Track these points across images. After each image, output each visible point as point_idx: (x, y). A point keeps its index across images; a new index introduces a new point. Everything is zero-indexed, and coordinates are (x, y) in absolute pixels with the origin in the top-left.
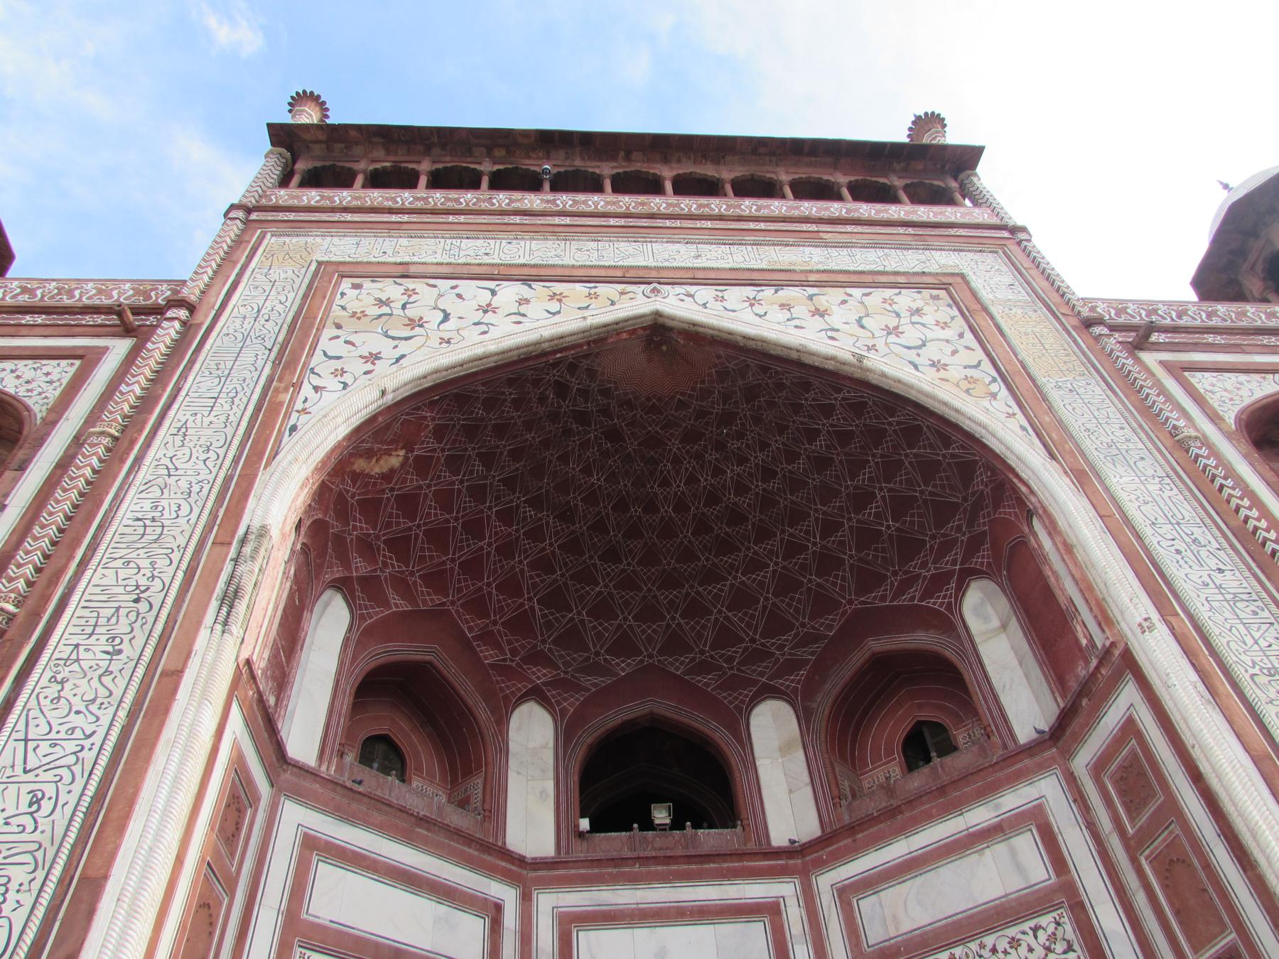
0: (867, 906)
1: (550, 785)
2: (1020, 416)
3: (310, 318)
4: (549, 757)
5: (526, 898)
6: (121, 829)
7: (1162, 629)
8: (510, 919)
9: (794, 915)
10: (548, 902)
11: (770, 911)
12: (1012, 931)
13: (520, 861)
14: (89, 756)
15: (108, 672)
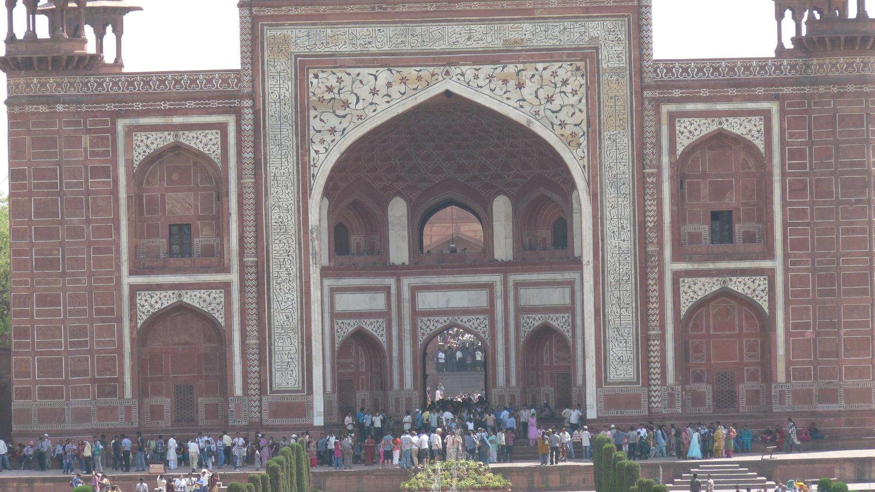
0: (522, 291)
1: (406, 233)
2: (586, 159)
3: (302, 104)
4: (405, 220)
5: (398, 282)
6: (311, 325)
7: (591, 265)
8: (393, 290)
9: (499, 288)
10: (407, 282)
11: (490, 286)
12: (557, 315)
13: (395, 267)
14: (295, 305)
15: (290, 281)
